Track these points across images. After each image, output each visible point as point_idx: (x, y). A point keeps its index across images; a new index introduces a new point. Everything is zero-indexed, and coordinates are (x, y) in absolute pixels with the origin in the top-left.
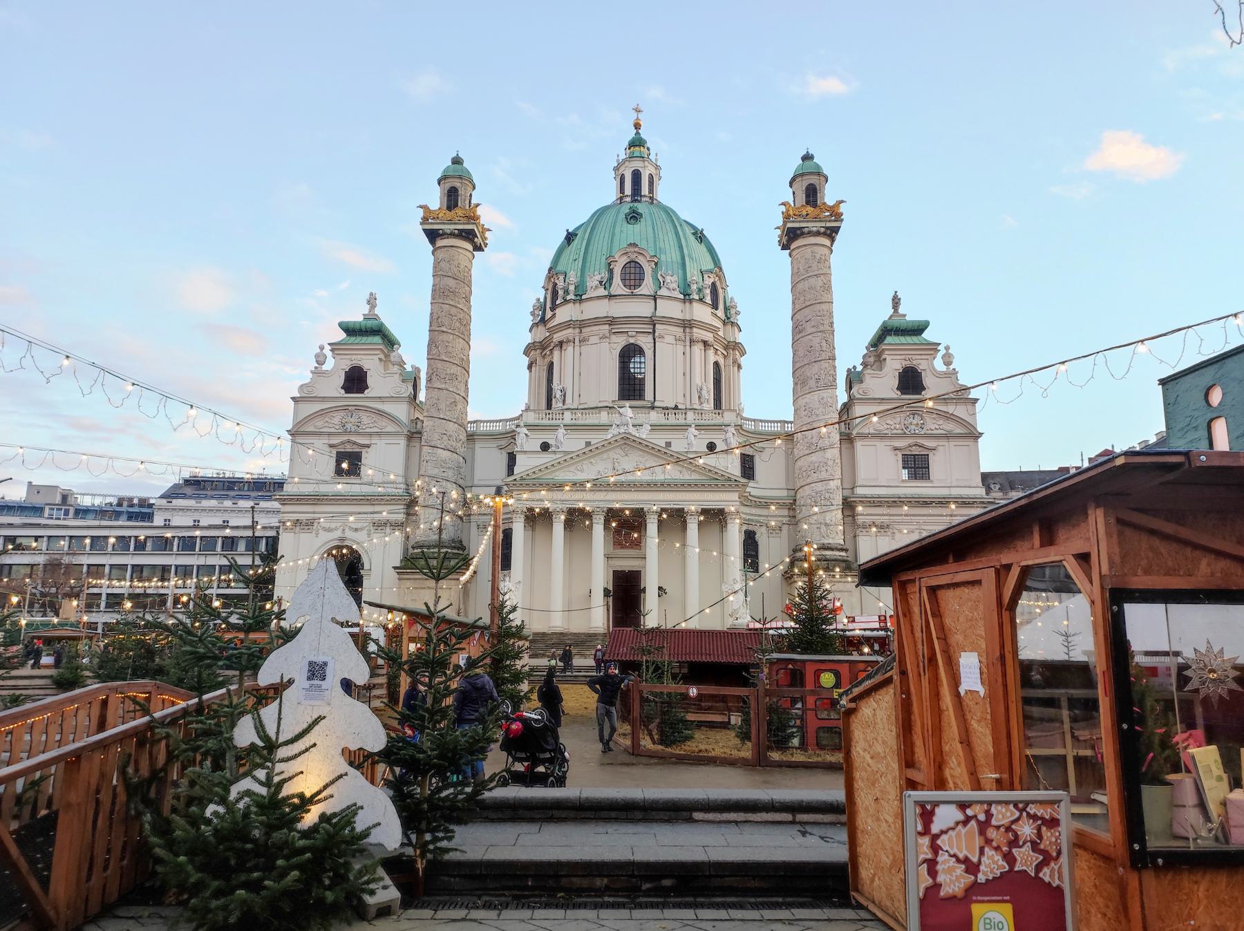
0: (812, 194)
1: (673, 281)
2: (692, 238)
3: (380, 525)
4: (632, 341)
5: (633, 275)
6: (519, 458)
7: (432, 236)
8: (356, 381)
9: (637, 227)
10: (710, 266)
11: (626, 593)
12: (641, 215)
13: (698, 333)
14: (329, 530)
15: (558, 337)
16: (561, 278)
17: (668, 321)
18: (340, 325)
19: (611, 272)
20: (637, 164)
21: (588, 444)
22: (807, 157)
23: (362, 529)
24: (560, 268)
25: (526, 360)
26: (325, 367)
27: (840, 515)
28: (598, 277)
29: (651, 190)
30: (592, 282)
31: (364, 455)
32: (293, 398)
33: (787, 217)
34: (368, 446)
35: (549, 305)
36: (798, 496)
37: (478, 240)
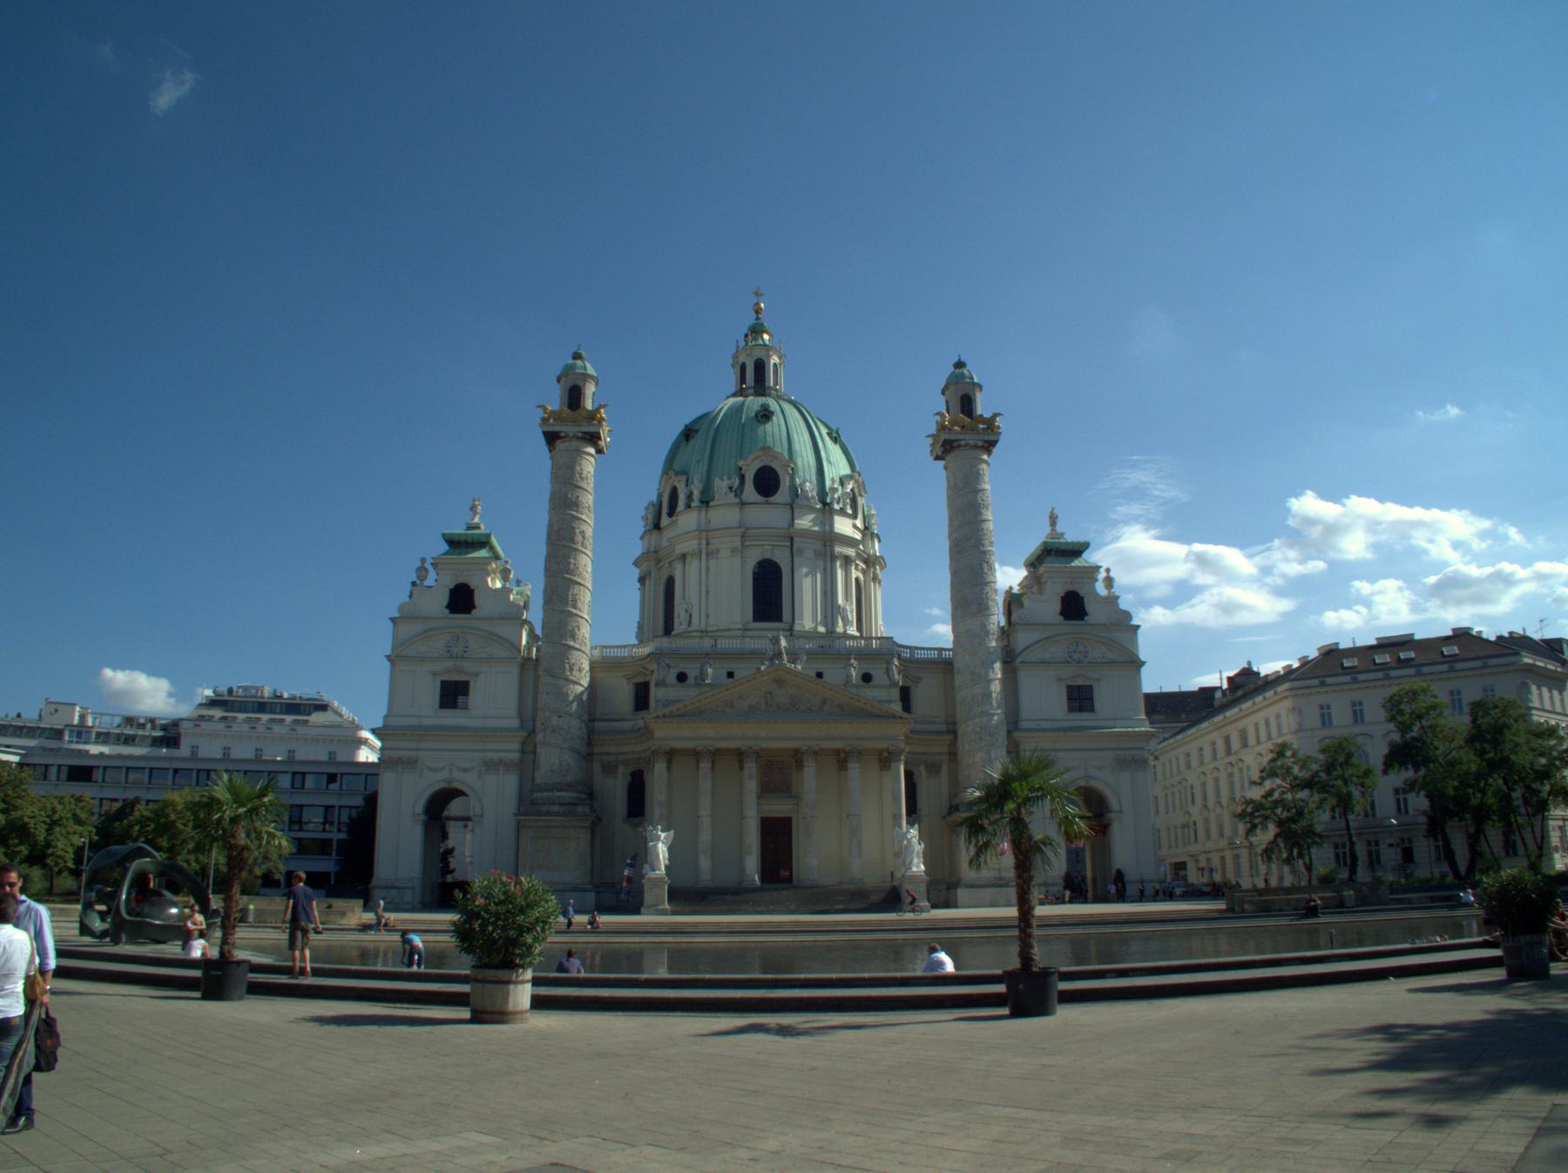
0: (967, 404)
1: (810, 488)
2: (827, 439)
3: (491, 766)
4: (768, 556)
5: (767, 482)
6: (655, 693)
7: (551, 438)
8: (462, 599)
9: (768, 427)
10: (845, 470)
11: (777, 838)
12: (772, 413)
13: (838, 549)
14: (435, 770)
15: (681, 548)
16: (684, 478)
17: (805, 533)
18: (444, 535)
19: (742, 478)
20: (759, 354)
21: (730, 675)
22: (960, 365)
23: (472, 769)
24: (677, 467)
25: (636, 573)
26: (426, 583)
27: (1004, 753)
28: (725, 484)
29: (776, 383)
30: (721, 485)
31: (472, 686)
32: (393, 620)
33: (942, 428)
34: (477, 675)
35: (665, 510)
36: (960, 732)
37: (602, 443)
